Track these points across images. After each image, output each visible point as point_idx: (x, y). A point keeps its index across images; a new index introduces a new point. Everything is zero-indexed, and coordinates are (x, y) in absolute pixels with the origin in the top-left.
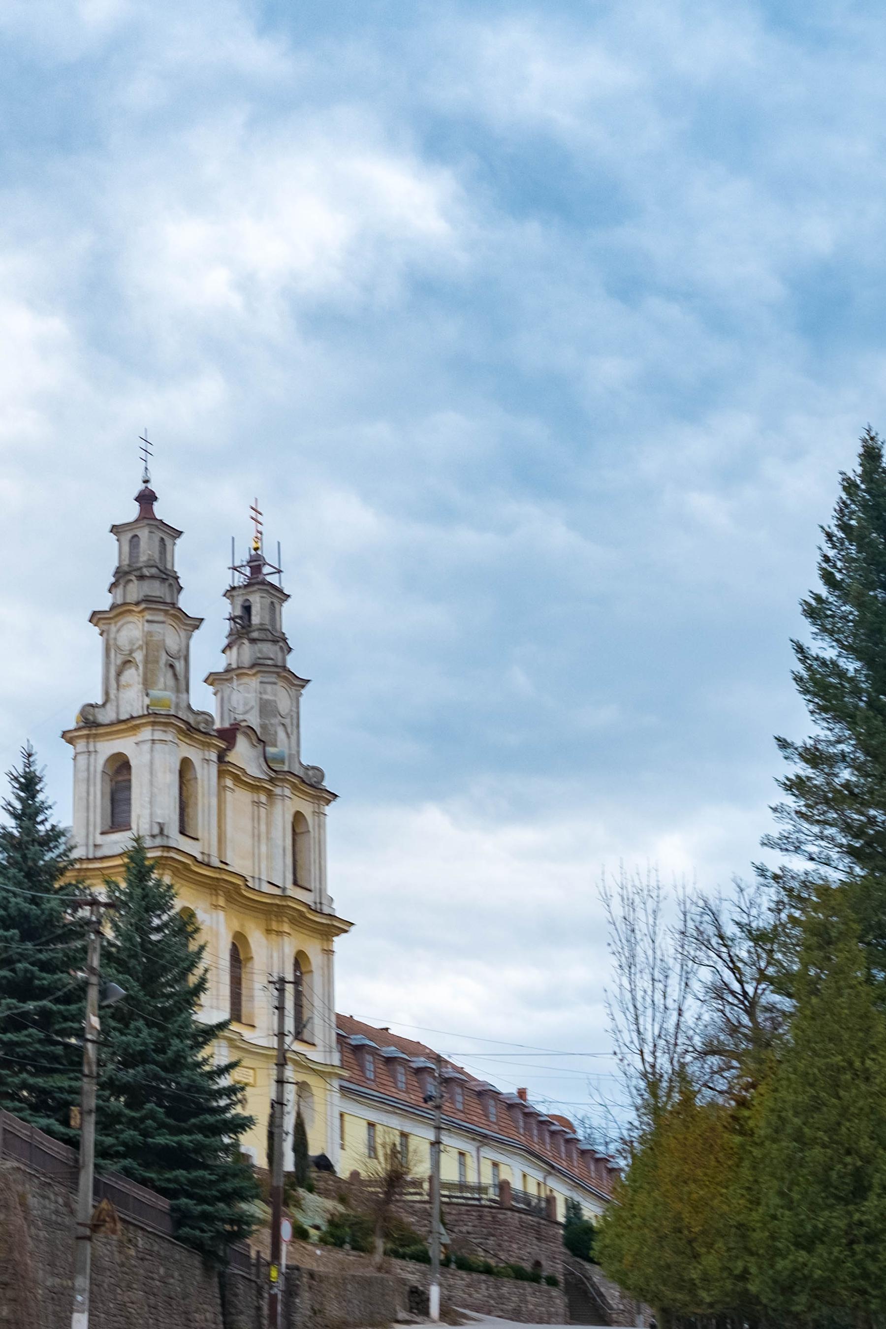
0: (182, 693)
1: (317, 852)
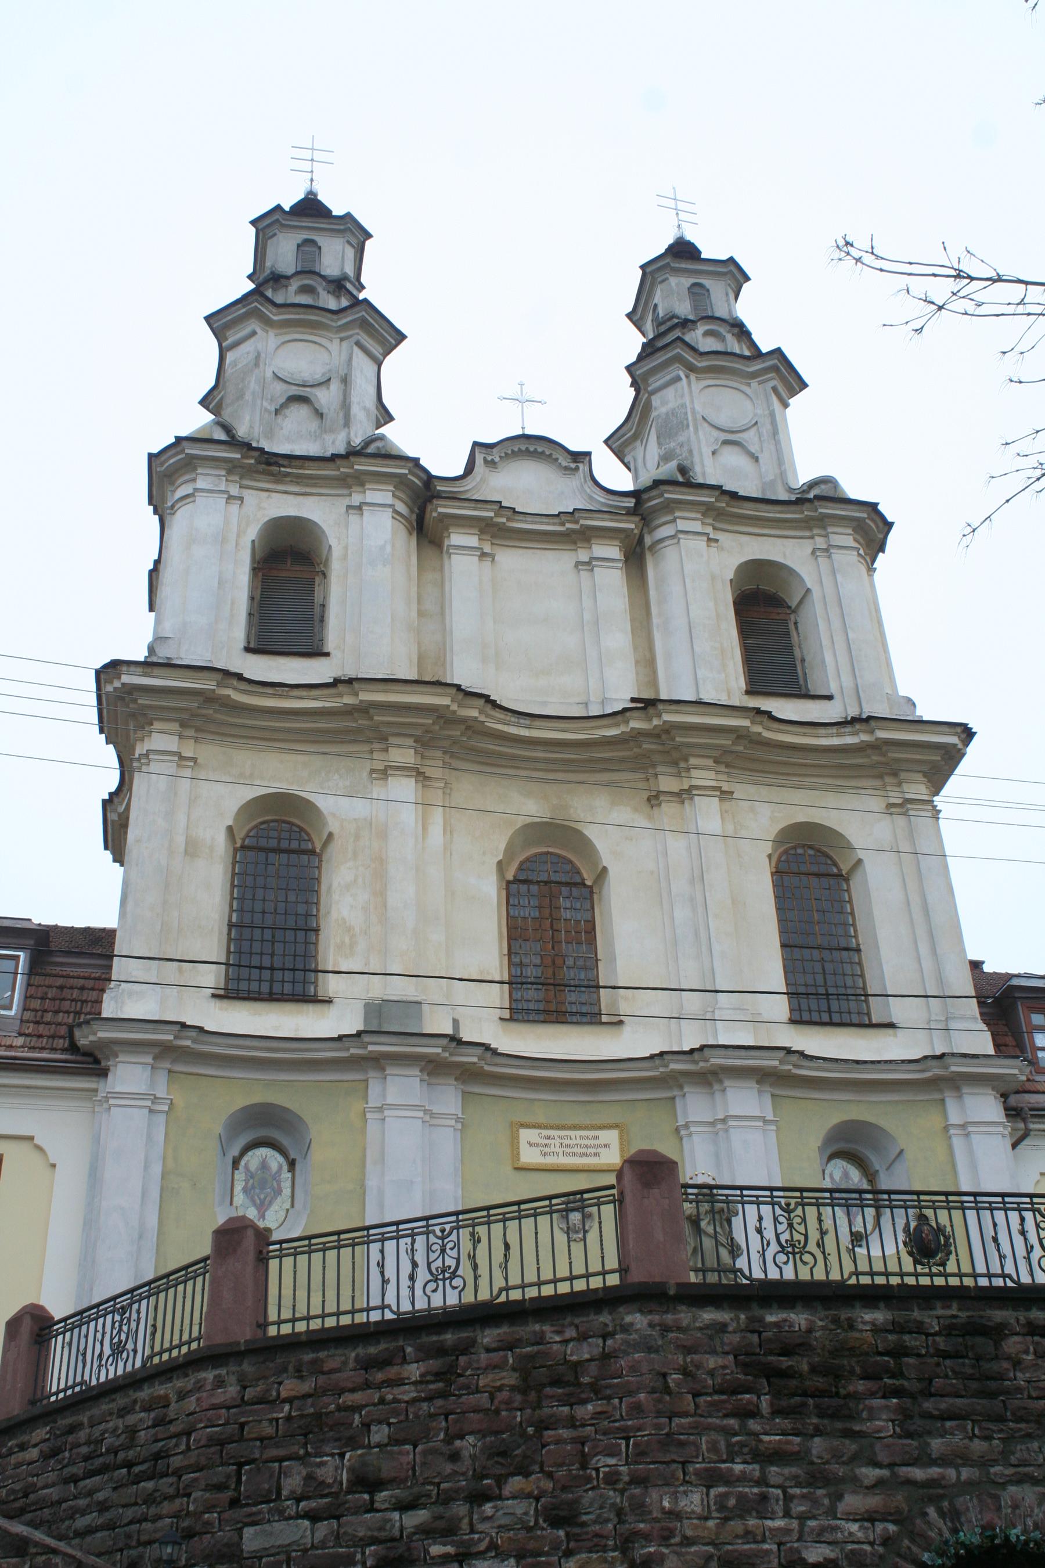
0: (332, 431)
1: (836, 624)
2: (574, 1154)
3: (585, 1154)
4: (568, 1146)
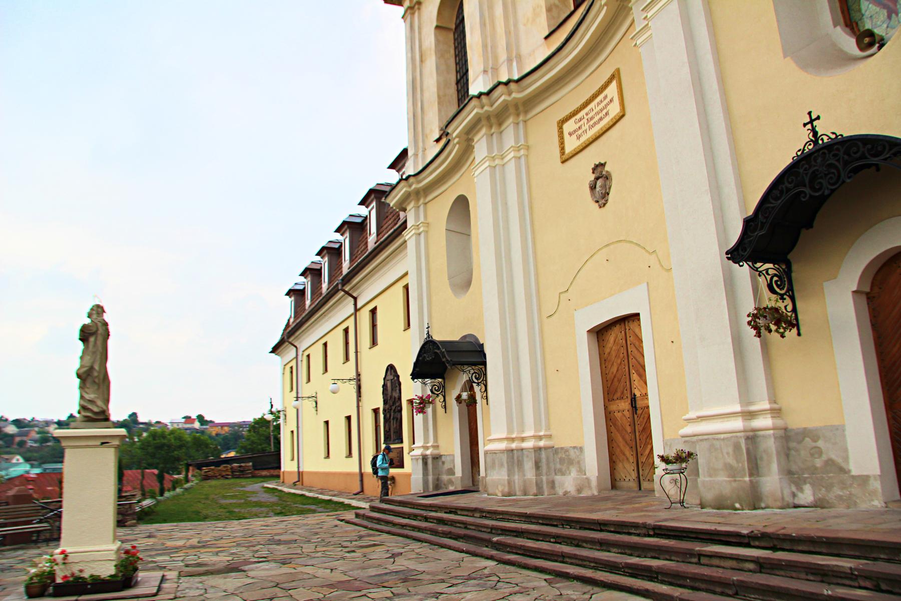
2: (595, 124)
3: (601, 119)
4: (592, 118)
